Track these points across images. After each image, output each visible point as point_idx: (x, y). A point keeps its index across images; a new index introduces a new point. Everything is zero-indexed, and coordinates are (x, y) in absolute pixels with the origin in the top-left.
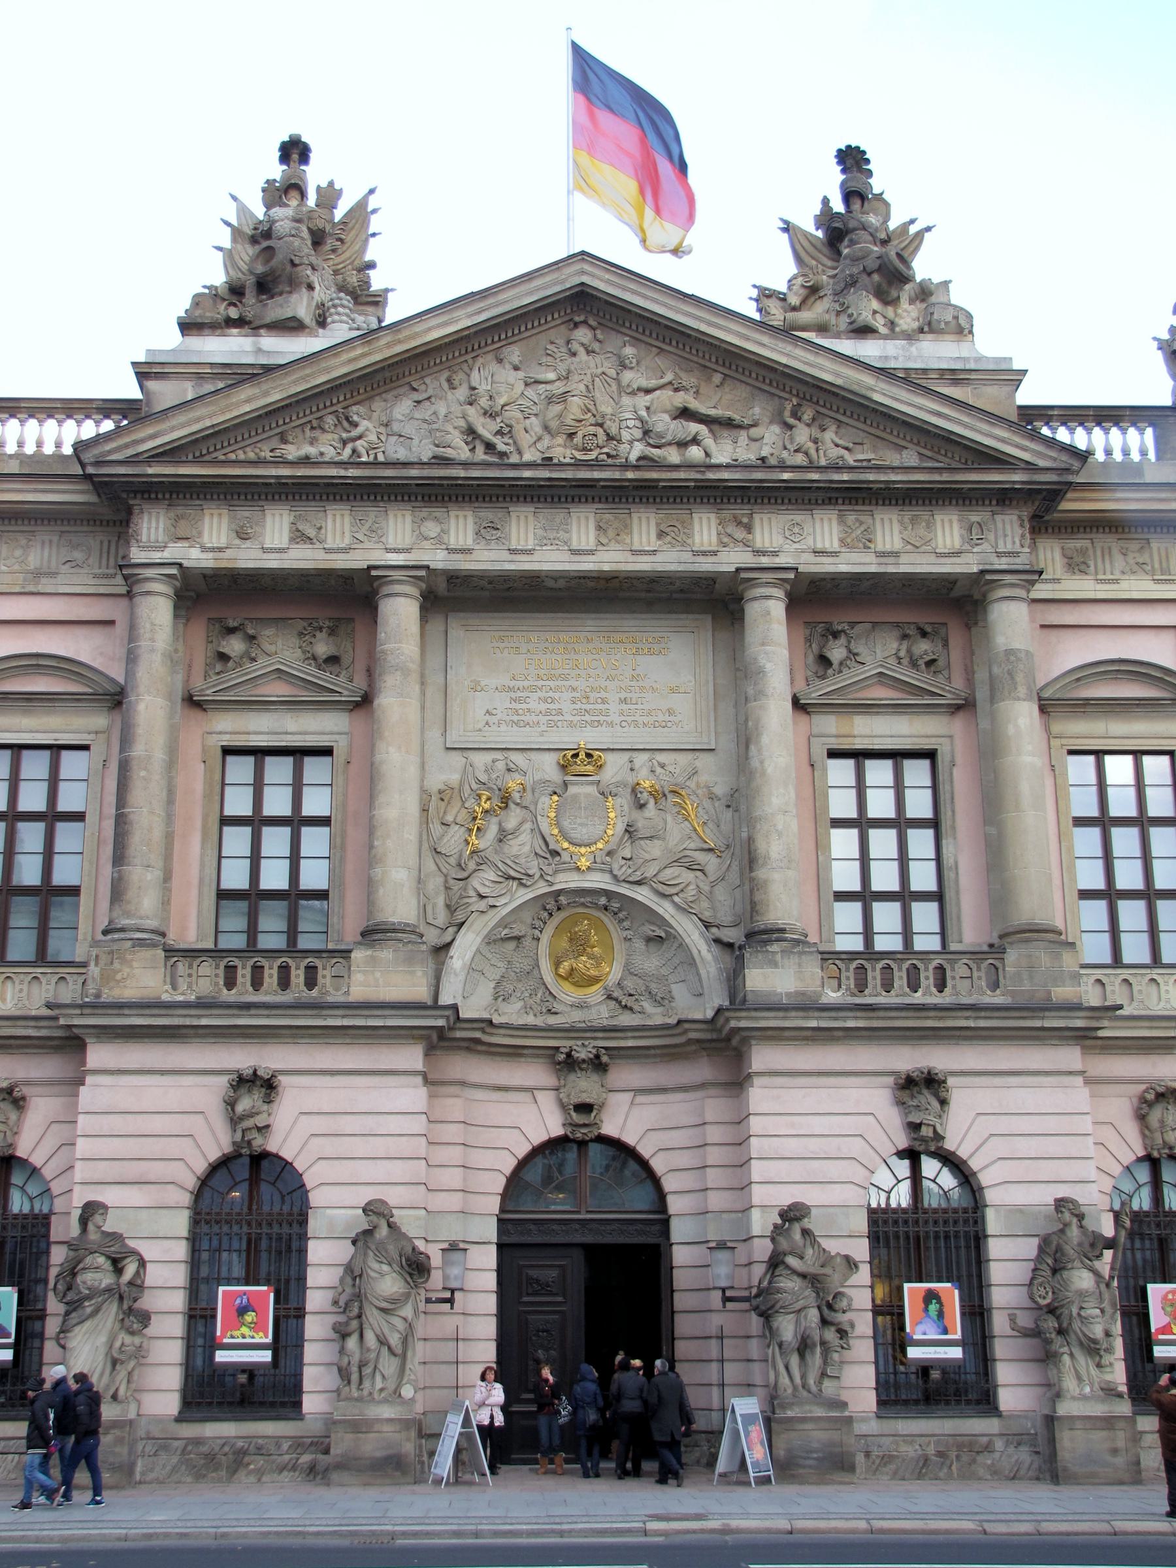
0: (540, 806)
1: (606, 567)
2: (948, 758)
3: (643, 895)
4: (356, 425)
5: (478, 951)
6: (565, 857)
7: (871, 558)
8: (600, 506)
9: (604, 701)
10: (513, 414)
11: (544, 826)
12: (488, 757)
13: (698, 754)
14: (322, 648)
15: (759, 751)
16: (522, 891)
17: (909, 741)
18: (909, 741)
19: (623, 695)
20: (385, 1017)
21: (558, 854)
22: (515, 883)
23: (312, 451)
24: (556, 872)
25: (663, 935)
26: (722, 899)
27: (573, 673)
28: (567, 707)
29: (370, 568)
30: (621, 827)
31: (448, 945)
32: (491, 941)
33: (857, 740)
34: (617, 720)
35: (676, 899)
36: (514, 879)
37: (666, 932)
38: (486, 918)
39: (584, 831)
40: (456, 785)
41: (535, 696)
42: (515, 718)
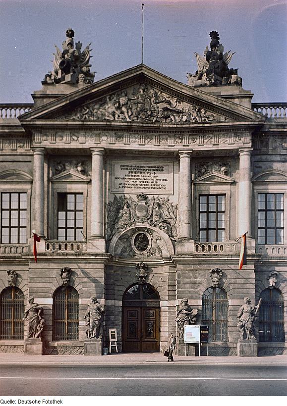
1: (147, 149)
4: (86, 110)
7: (212, 146)
9: (148, 182)
10: (124, 109)
14: (79, 169)
19: (152, 181)
23: (74, 117)
27: (140, 175)
28: (139, 183)
29: (90, 148)
31: (110, 240)
32: (120, 239)
34: (150, 187)
40: (112, 201)
41: (131, 180)
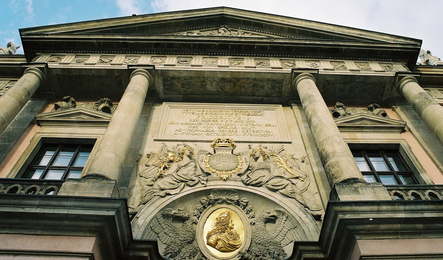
0: (201, 158)
2: (407, 146)
3: (262, 191)
5: (155, 217)
6: (214, 175)
8: (231, 57)
11: (203, 166)
12: (175, 144)
13: (283, 144)
15: (318, 117)
16: (187, 188)
17: (385, 141)
18: (385, 141)
20: (70, 207)
21: (210, 174)
22: (183, 184)
24: (207, 181)
25: (275, 214)
26: (309, 198)
30: (245, 167)
33: (360, 140)
35: (280, 191)
36: (182, 181)
37: (277, 211)
38: (163, 200)
39: (225, 164)
42: (190, 132)
